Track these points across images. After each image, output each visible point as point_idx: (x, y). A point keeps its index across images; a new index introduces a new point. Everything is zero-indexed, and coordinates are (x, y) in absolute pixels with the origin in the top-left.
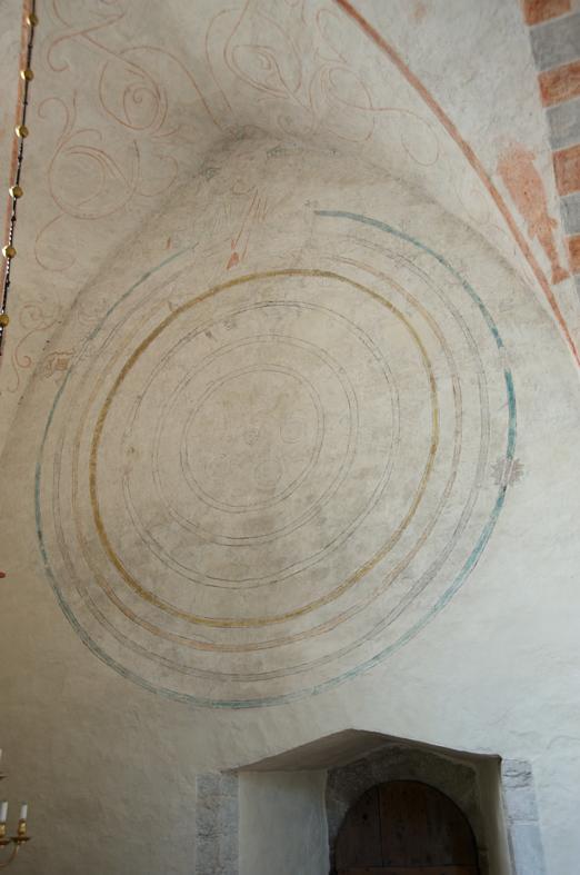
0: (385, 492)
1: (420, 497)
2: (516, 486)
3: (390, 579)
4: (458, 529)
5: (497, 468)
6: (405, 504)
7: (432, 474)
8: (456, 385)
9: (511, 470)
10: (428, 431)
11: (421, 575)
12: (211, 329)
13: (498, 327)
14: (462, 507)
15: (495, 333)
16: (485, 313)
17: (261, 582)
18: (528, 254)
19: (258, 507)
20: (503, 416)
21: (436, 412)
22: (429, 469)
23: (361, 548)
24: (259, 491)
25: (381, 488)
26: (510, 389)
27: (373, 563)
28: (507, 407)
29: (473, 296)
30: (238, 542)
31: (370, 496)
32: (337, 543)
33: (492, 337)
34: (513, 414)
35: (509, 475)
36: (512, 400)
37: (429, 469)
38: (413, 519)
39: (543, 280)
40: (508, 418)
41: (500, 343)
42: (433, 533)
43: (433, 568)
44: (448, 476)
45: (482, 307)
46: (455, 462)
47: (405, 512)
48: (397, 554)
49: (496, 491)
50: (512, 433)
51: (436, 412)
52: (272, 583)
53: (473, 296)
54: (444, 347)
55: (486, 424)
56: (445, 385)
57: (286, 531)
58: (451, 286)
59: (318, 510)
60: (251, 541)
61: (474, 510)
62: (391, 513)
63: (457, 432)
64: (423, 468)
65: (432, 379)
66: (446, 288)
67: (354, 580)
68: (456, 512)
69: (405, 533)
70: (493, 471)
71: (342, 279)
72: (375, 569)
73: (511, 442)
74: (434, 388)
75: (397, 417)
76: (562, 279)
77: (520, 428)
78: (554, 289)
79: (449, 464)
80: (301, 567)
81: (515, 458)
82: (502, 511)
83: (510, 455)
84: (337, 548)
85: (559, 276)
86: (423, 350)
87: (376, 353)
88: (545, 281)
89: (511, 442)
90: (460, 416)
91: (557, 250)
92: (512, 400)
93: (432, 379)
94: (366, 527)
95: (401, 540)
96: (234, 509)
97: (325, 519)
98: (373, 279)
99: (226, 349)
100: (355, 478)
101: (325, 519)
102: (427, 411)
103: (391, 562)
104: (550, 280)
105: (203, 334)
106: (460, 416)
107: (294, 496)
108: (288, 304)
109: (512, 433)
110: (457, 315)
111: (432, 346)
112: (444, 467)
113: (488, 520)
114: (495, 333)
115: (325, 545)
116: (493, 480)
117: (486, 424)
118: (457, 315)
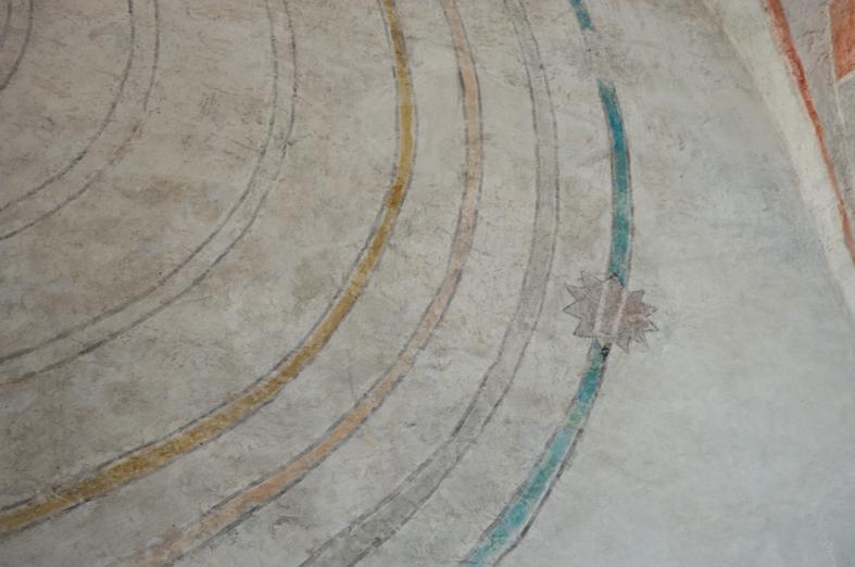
0: (230, 260)
1: (349, 304)
2: (637, 354)
3: (229, 514)
4: (468, 420)
5: (583, 295)
6: (298, 311)
7: (387, 256)
8: (467, 68)
9: (616, 314)
10: (383, 148)
11: (343, 525)
14: (485, 364)
20: (598, 180)
21: (406, 113)
22: (379, 240)
23: (127, 397)
25: (218, 247)
26: (615, 124)
27: (170, 451)
28: (606, 163)
32: (31, 363)
34: (621, 181)
35: (616, 323)
36: (620, 152)
37: (379, 240)
38: (324, 356)
40: (608, 188)
42: (386, 411)
43: (385, 509)
44: (438, 276)
46: (462, 244)
47: (298, 331)
48: (260, 444)
49: (579, 354)
50: (621, 226)
51: (406, 113)
55: (550, 186)
56: (434, 62)
61: (518, 383)
62: (251, 322)
63: (467, 177)
64: (360, 233)
65: (397, 34)
67: (92, 488)
68: (460, 375)
69: (292, 389)
70: (570, 300)
72: (176, 469)
73: (620, 247)
74: (401, 54)
75: (286, 86)
77: (643, 216)
79: (442, 248)
81: (632, 285)
82: (602, 406)
83: (616, 275)
84: (31, 375)
89: (620, 247)
92: (620, 152)
93: (397, 34)
94: (153, 341)
95: (279, 404)
100: (128, 195)
102: (380, 102)
103: (237, 462)
106: (476, 140)
109: (621, 226)
113: (558, 417)
116: (571, 323)
117: (550, 186)
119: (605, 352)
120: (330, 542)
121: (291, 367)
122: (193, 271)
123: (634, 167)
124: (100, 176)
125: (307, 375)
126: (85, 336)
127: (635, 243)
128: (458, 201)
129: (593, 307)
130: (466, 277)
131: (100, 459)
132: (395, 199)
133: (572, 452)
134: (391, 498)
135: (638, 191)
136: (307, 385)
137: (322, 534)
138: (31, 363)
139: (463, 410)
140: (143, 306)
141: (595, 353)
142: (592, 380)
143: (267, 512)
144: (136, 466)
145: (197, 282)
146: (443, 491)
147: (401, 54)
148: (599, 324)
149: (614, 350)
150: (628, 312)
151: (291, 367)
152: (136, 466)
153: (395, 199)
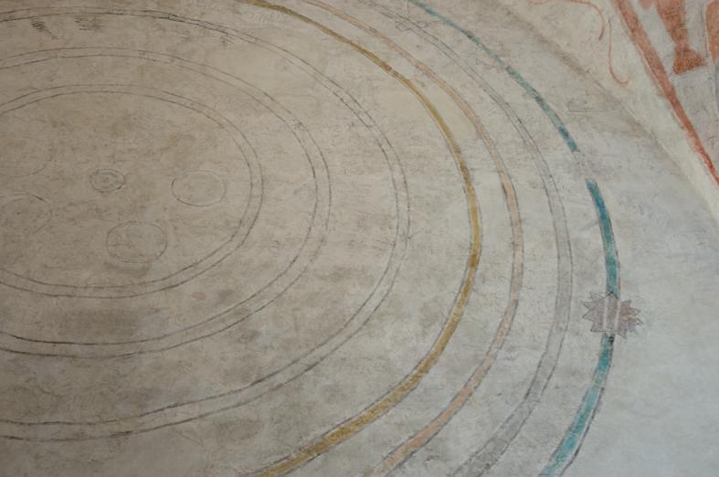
0: (382, 309)
1: (454, 326)
3: (399, 457)
4: (533, 389)
5: (593, 307)
6: (424, 334)
7: (472, 296)
8: (507, 182)
10: (463, 233)
11: (466, 458)
12: (44, 19)
13: (569, 128)
14: (539, 354)
15: (565, 134)
16: (546, 108)
17: (88, 430)
18: (635, 28)
19: (104, 293)
20: (594, 238)
21: (474, 212)
22: (467, 287)
23: (334, 393)
24: (109, 267)
25: (375, 302)
26: (600, 204)
27: (361, 422)
28: (597, 227)
29: (525, 85)
30: (44, 348)
31: (353, 311)
32: (280, 378)
33: (560, 138)
35: (616, 322)
36: (604, 221)
37: (467, 287)
38: (442, 359)
39: (655, 66)
40: (600, 242)
41: (573, 147)
42: (483, 388)
43: (490, 447)
44: (504, 305)
45: (539, 99)
46: (516, 284)
47: (426, 345)
48: (411, 414)
49: (596, 342)
50: (611, 263)
51: (474, 212)
52: (114, 435)
53: (525, 85)
54: (481, 133)
55: (565, 244)
56: (487, 181)
57: (164, 343)
58: (487, 67)
59: (243, 316)
60: (75, 349)
61: (561, 364)
62: (398, 343)
64: (455, 284)
65: (463, 168)
66: (479, 68)
67: (320, 447)
68: (526, 362)
69: (426, 380)
70: (586, 311)
71: (308, 20)
72: (366, 433)
73: (612, 275)
74: (467, 179)
75: (403, 206)
76: (691, 67)
77: (624, 256)
78: (675, 80)
79: (504, 288)
80: (194, 411)
81: (623, 298)
82: (614, 373)
83: (612, 292)
84: (280, 386)
85: (686, 61)
86: (445, 129)
87: (365, 118)
88: (660, 67)
89: (612, 275)
90: (517, 223)
91: (688, 26)
92: (604, 221)
93: (463, 168)
94: (344, 359)
95: (419, 390)
96: (44, 289)
97: (254, 335)
98: (360, 33)
99: (77, 53)
100: (322, 278)
101: (254, 335)
102: (459, 208)
103: (400, 425)
104: (669, 67)
105: (27, 23)
106: (517, 223)
107: (191, 288)
108: (205, 27)
109: (611, 263)
110: (497, 100)
111: (462, 132)
112: (494, 290)
113: (588, 382)
114: (565, 134)
115: (254, 378)
116: (587, 324)
117: (565, 244)
118: (497, 100)
119: (611, 340)
120: (460, 469)
121: (424, 367)
122: (362, 317)
123: (615, 228)
124: (306, 270)
125: (433, 371)
126: (309, 360)
127: (621, 273)
128: (511, 260)
129: (600, 313)
130: (521, 304)
131: (323, 430)
132: (473, 262)
133: (599, 403)
134: (492, 439)
135: (619, 242)
136: (435, 376)
137: (454, 464)
138: (280, 378)
139: (529, 383)
140: (337, 340)
141: (606, 341)
142: (606, 357)
143: (421, 454)
144: (343, 432)
145: (365, 323)
146: (523, 433)
147: (467, 179)
148: (605, 323)
149: (617, 338)
150: (622, 314)
151: (424, 367)
152: (343, 432)
153: (473, 262)
